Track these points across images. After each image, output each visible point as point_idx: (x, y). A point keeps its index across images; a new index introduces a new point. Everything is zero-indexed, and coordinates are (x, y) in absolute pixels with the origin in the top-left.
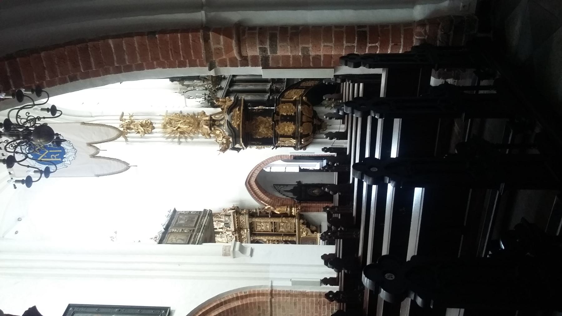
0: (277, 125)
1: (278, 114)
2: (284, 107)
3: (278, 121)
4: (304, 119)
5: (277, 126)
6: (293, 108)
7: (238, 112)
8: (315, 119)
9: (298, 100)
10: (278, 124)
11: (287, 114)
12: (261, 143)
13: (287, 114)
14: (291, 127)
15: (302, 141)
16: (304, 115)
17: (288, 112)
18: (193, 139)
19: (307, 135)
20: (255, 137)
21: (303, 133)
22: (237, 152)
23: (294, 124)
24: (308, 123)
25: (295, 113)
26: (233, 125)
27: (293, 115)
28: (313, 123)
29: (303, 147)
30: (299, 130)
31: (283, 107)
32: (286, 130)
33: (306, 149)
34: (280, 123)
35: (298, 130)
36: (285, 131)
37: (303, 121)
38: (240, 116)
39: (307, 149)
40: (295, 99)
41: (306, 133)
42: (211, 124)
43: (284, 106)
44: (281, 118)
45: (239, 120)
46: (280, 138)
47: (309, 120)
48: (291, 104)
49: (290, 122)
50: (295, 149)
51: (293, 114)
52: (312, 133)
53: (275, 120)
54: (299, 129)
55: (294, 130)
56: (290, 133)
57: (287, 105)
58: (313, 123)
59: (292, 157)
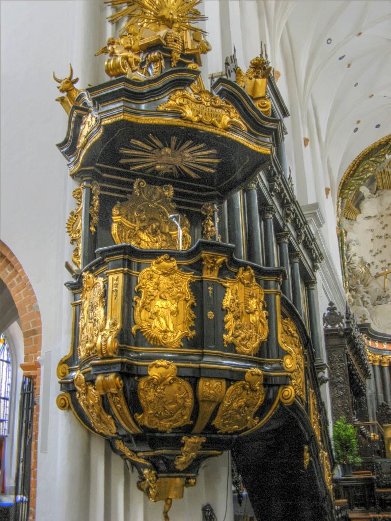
0: (179, 265)
1: (224, 270)
2: (253, 303)
3: (198, 267)
4: (208, 387)
5: (174, 264)
6: (250, 338)
7: (226, 119)
8: (204, 440)
9: (280, 363)
10: (185, 269)
11: (225, 311)
12: (92, 229)
13: (225, 311)
14: (171, 328)
15: (106, 374)
16: (228, 387)
17: (237, 318)
18: (112, 21)
19: (134, 405)
20: (115, 211)
21: (142, 384)
22: (61, 140)
23: (185, 339)
24: (189, 402)
25: (232, 347)
26: (178, 93)
27: (224, 336)
28: (188, 430)
29: (73, 392)
30: (159, 362)
31: (254, 300)
32: (159, 303)
33: (63, 407)
34: (189, 277)
35: (164, 358)
36: (152, 298)
37: (201, 383)
38: (213, 125)
39: (61, 413)
40: (288, 353)
41: (148, 395)
42: (170, 52)
43: (258, 304)
44: (213, 283)
45: (196, 119)
46: (121, 276)
47: (206, 410)
48: (266, 333)
49: (192, 324)
50: (63, 362)
51: (228, 337)
52: (143, 427)
53: (204, 254)
54: (165, 363)
55: (156, 339)
56: (141, 317)
57: (261, 316)
58: (188, 430)
59: (32, 373)
